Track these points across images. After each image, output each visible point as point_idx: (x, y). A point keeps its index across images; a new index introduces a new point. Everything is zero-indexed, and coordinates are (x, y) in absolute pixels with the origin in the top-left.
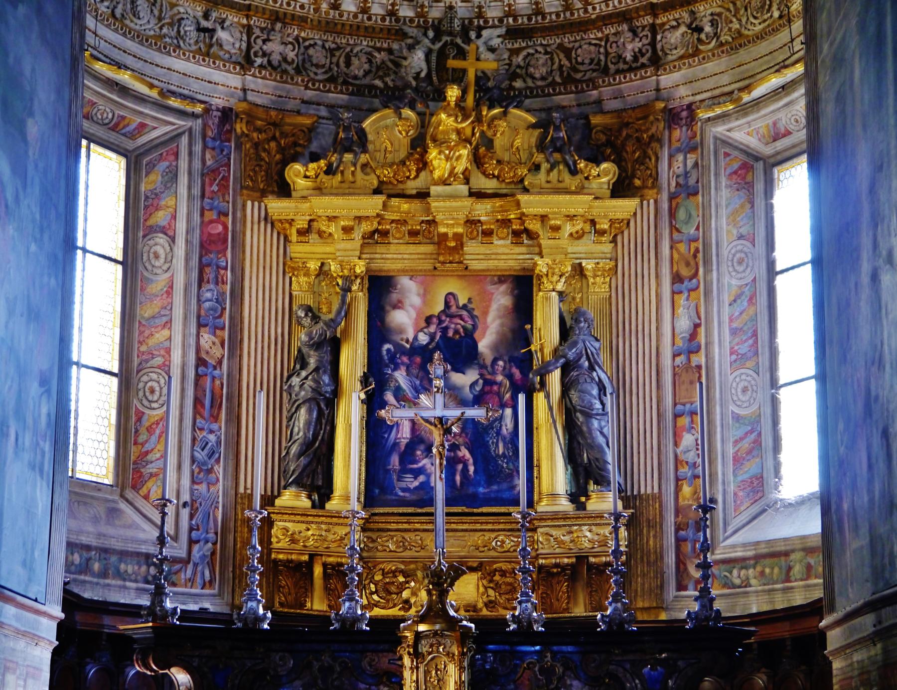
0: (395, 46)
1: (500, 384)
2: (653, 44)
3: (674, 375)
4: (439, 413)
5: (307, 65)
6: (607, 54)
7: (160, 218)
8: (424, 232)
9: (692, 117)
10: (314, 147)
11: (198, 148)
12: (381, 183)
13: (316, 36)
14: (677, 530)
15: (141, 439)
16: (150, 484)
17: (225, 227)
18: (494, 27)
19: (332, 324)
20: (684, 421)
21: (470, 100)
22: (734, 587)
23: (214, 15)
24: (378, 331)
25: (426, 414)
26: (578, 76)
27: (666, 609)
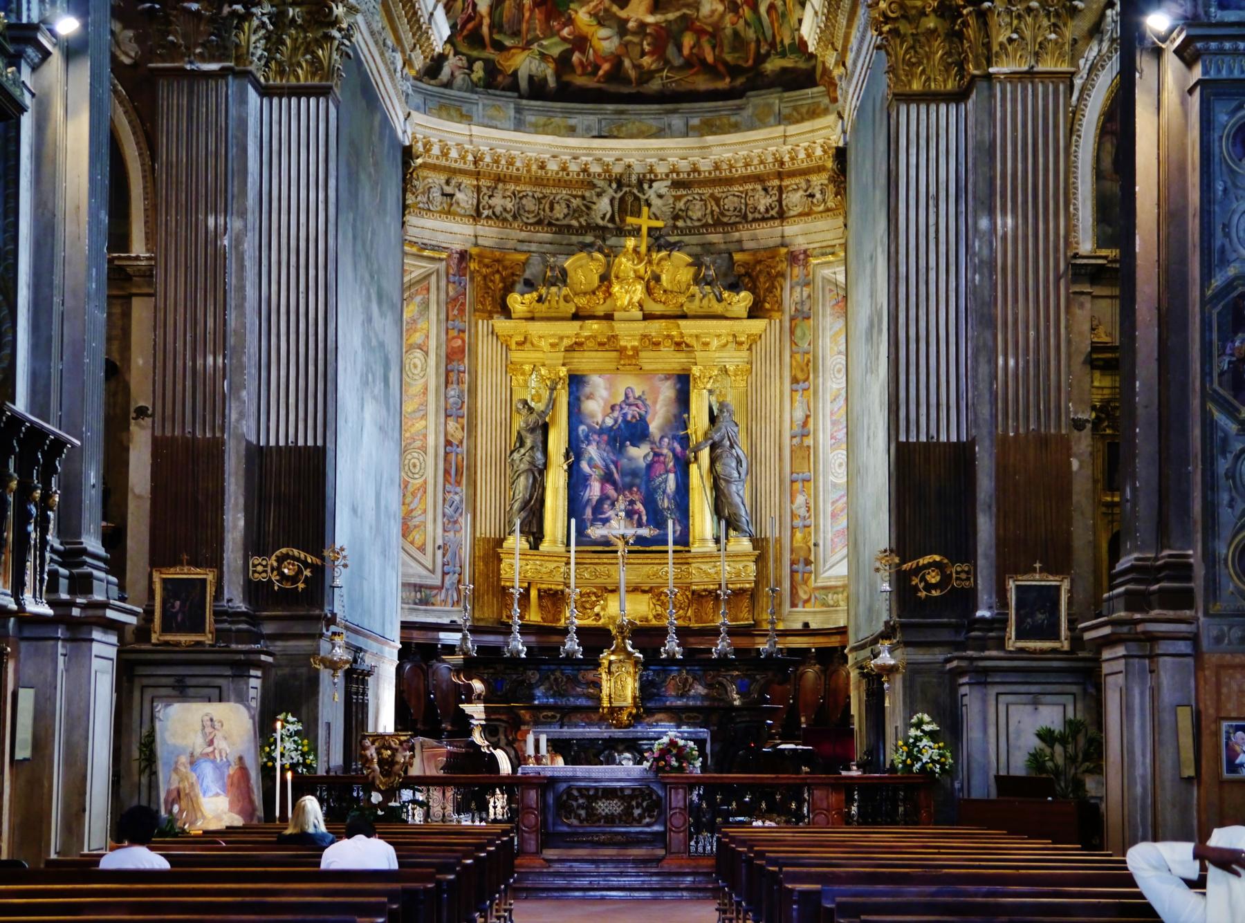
0: (587, 194)
1: (665, 456)
2: (780, 201)
3: (792, 451)
4: (622, 532)
5: (522, 212)
6: (746, 205)
7: (418, 338)
8: (609, 343)
9: (806, 265)
10: (527, 275)
11: (443, 283)
12: (578, 308)
13: (528, 189)
14: (792, 564)
15: (407, 501)
16: (414, 533)
17: (464, 341)
18: (662, 180)
19: (543, 414)
20: (798, 485)
21: (643, 249)
22: (829, 606)
23: (453, 182)
24: (575, 414)
25: (614, 532)
26: (725, 220)
27: (783, 620)
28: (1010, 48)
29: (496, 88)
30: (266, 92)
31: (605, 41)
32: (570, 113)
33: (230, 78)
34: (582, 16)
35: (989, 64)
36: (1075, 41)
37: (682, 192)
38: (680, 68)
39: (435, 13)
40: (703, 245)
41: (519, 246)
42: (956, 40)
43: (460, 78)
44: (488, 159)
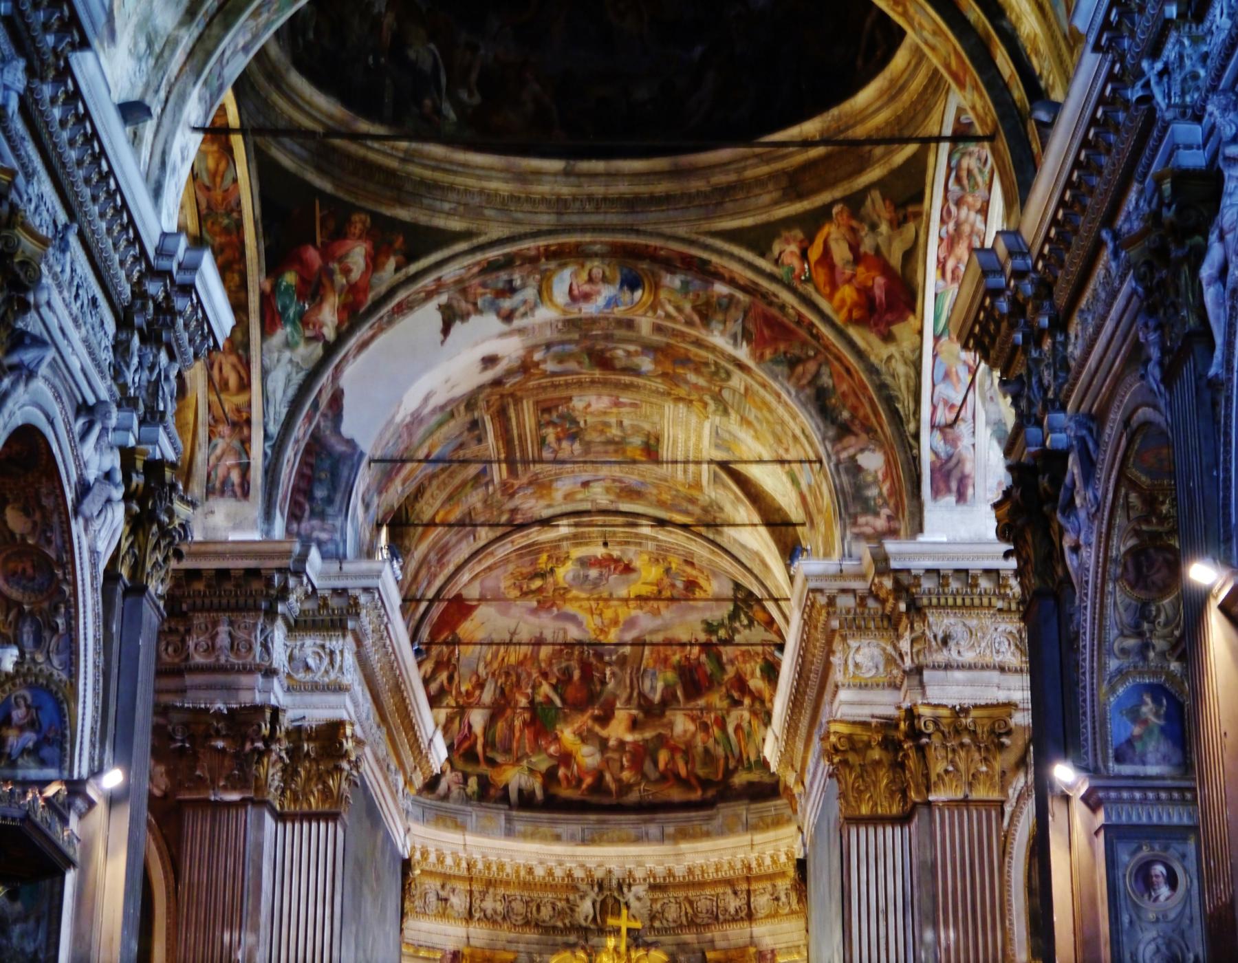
0: (571, 897)
6: (717, 907)
21: (623, 948)
23: (448, 887)
26: (699, 921)
28: (946, 779)
29: (488, 801)
30: (280, 817)
31: (587, 756)
32: (554, 822)
33: (249, 807)
34: (567, 734)
35: (928, 790)
36: (1004, 773)
37: (658, 895)
38: (657, 782)
39: (435, 740)
40: (678, 945)
41: (508, 946)
42: (899, 770)
43: (455, 790)
44: (480, 866)
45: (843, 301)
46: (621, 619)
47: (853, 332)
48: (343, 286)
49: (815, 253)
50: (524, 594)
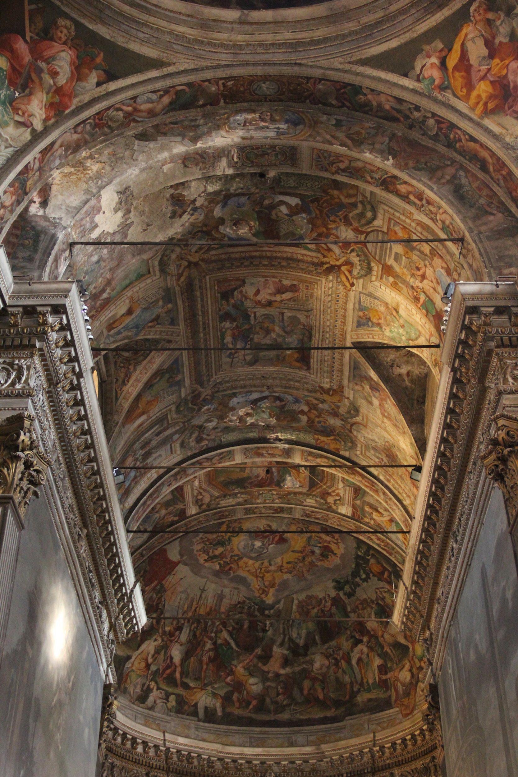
29: (183, 714)
34: (240, 669)
45: (479, 96)
46: (277, 581)
47: (488, 122)
48: (51, 87)
49: (452, 61)
50: (211, 559)
